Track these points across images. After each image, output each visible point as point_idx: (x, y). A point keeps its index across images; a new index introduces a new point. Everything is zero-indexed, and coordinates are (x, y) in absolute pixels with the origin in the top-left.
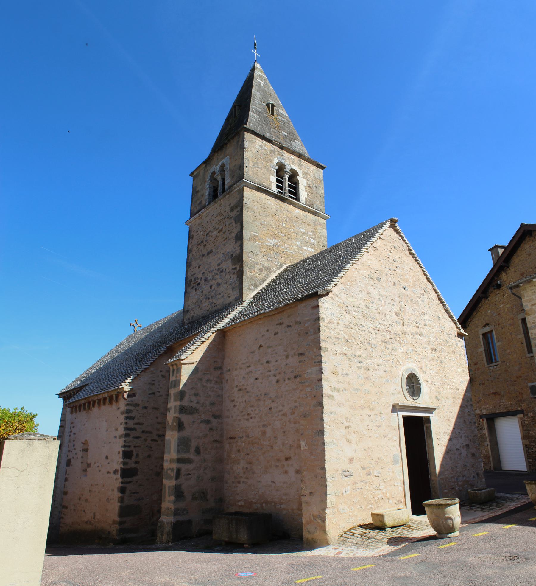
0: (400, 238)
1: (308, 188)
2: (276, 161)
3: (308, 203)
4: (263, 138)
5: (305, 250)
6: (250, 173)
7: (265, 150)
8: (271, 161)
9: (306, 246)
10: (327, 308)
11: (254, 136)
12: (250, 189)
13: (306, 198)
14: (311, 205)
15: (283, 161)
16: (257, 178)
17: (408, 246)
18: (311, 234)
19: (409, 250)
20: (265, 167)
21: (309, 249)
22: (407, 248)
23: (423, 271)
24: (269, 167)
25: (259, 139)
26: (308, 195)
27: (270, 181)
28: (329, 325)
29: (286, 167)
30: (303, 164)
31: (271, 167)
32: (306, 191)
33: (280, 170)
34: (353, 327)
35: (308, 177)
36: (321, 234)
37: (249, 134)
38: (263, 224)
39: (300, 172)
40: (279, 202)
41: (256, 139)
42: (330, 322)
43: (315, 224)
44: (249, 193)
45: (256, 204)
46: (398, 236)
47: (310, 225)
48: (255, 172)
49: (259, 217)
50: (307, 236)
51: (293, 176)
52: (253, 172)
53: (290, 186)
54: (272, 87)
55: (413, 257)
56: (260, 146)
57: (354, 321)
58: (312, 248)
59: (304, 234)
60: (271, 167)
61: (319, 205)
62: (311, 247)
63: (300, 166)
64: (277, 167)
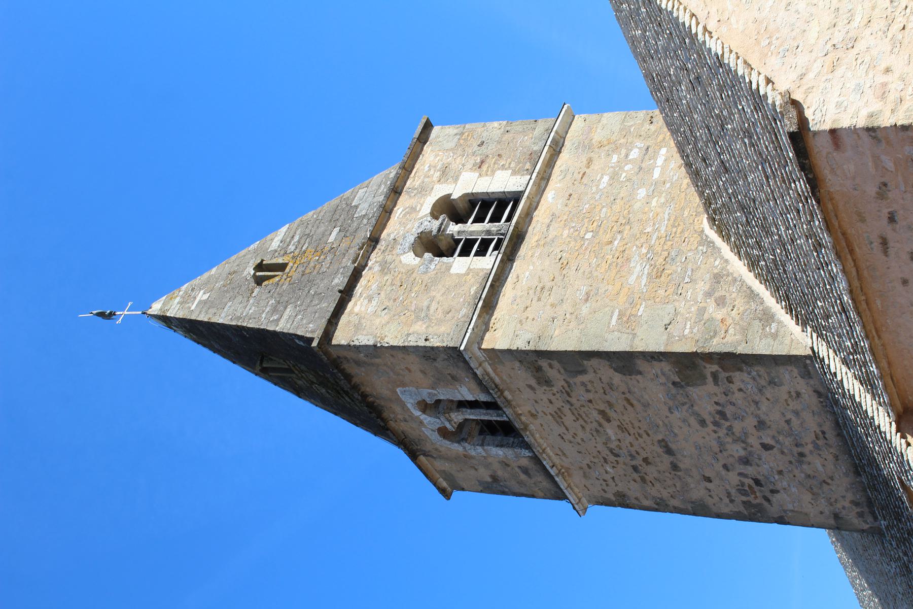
1: (484, 167)
2: (410, 259)
3: (528, 166)
4: (347, 294)
5: (662, 173)
6: (443, 329)
7: (380, 288)
8: (411, 271)
9: (650, 171)
10: (838, 105)
12: (487, 330)
13: (514, 173)
14: (533, 158)
15: (411, 239)
16: (458, 311)
18: (615, 158)
21: (660, 162)
24: (425, 278)
26: (503, 167)
27: (467, 274)
28: (892, 97)
29: (428, 228)
30: (417, 183)
32: (493, 172)
33: (434, 246)
34: (896, 26)
37: (337, 333)
39: (440, 191)
40: (524, 250)
41: (351, 312)
42: (883, 96)
43: (586, 146)
44: (498, 334)
45: (530, 313)
47: (590, 161)
48: (440, 314)
49: (567, 307)
50: (621, 168)
51: (452, 209)
52: (440, 322)
53: (479, 219)
56: (370, 301)
57: (878, 24)
59: (614, 177)
60: (426, 273)
62: (654, 158)
63: (423, 190)
64: (428, 255)
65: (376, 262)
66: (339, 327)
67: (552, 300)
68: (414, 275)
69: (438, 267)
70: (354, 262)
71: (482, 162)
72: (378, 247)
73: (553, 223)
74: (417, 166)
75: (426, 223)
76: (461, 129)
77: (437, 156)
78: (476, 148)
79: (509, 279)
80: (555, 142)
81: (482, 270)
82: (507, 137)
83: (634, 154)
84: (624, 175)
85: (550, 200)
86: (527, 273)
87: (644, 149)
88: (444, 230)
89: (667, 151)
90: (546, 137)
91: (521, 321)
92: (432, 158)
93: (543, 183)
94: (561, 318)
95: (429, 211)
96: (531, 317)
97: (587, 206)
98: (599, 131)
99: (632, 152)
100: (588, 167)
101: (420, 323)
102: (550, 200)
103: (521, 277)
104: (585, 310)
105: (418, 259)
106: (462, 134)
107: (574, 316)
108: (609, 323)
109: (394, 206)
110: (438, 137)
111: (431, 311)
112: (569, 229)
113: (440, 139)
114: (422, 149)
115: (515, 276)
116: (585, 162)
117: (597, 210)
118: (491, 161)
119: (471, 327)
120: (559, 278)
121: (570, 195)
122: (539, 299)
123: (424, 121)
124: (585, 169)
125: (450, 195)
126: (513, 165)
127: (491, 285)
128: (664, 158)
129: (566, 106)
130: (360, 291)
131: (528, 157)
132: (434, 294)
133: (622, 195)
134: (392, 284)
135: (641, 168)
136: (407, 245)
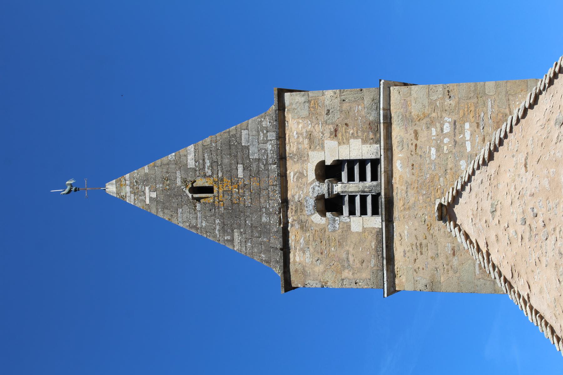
0: (468, 188)
1: (339, 135)
2: (317, 218)
3: (371, 135)
4: (286, 249)
7: (307, 243)
8: (323, 230)
9: (463, 145)
11: (292, 268)
12: (394, 276)
13: (364, 142)
14: (374, 127)
15: (312, 202)
16: (370, 262)
17: (478, 168)
18: (434, 131)
19: (485, 163)
20: (340, 244)
21: (468, 136)
22: (483, 168)
23: (518, 121)
24: (336, 235)
25: (291, 255)
26: (354, 136)
30: (294, 149)
31: (334, 231)
32: (348, 140)
33: (331, 205)
35: (315, 134)
36: (426, 103)
37: (293, 278)
38: (453, 249)
39: (315, 158)
40: (396, 214)
41: (295, 261)
43: (408, 119)
44: (404, 279)
45: (418, 264)
46: (465, 194)
47: (416, 133)
48: (358, 265)
50: (442, 141)
51: (329, 172)
53: (351, 178)
54: (142, 165)
55: (496, 149)
56: (304, 252)
58: (462, 127)
59: (439, 149)
61: (362, 105)
62: (462, 132)
63: (302, 157)
64: (328, 214)
65: (294, 220)
66: (291, 274)
67: (430, 254)
68: (327, 233)
69: (341, 226)
70: (280, 224)
71: (336, 131)
72: (290, 206)
73: (409, 189)
74: (287, 132)
75: (317, 188)
76: (306, 96)
77: (298, 123)
78: (326, 117)
79: (395, 237)
80: (385, 117)
81: (374, 228)
82: (345, 106)
83: (447, 128)
84: (445, 148)
86: (406, 232)
87: (452, 123)
88: (332, 192)
89: (470, 126)
90: (374, 107)
91: (415, 270)
92: (296, 125)
93: (389, 153)
94: (441, 267)
96: (421, 268)
97: (428, 176)
98: (413, 104)
99: (445, 127)
100: (417, 140)
101: (347, 271)
103: (403, 235)
104: (455, 262)
105: (324, 219)
106: (309, 102)
107: (449, 267)
108: (475, 272)
109: (286, 170)
110: (291, 104)
111: (351, 262)
112: (423, 196)
113: (294, 106)
114: (284, 117)
115: (398, 235)
116: (413, 135)
117: (436, 179)
118: (342, 129)
119: (385, 280)
120: (429, 237)
121: (413, 165)
122: (421, 254)
124: (415, 142)
125: (323, 162)
126: (360, 134)
127: (387, 246)
128: (469, 132)
129: (382, 82)
130: (293, 244)
131: (368, 126)
132: (347, 248)
133: (450, 166)
134: (314, 240)
135: (455, 142)
136: (311, 208)
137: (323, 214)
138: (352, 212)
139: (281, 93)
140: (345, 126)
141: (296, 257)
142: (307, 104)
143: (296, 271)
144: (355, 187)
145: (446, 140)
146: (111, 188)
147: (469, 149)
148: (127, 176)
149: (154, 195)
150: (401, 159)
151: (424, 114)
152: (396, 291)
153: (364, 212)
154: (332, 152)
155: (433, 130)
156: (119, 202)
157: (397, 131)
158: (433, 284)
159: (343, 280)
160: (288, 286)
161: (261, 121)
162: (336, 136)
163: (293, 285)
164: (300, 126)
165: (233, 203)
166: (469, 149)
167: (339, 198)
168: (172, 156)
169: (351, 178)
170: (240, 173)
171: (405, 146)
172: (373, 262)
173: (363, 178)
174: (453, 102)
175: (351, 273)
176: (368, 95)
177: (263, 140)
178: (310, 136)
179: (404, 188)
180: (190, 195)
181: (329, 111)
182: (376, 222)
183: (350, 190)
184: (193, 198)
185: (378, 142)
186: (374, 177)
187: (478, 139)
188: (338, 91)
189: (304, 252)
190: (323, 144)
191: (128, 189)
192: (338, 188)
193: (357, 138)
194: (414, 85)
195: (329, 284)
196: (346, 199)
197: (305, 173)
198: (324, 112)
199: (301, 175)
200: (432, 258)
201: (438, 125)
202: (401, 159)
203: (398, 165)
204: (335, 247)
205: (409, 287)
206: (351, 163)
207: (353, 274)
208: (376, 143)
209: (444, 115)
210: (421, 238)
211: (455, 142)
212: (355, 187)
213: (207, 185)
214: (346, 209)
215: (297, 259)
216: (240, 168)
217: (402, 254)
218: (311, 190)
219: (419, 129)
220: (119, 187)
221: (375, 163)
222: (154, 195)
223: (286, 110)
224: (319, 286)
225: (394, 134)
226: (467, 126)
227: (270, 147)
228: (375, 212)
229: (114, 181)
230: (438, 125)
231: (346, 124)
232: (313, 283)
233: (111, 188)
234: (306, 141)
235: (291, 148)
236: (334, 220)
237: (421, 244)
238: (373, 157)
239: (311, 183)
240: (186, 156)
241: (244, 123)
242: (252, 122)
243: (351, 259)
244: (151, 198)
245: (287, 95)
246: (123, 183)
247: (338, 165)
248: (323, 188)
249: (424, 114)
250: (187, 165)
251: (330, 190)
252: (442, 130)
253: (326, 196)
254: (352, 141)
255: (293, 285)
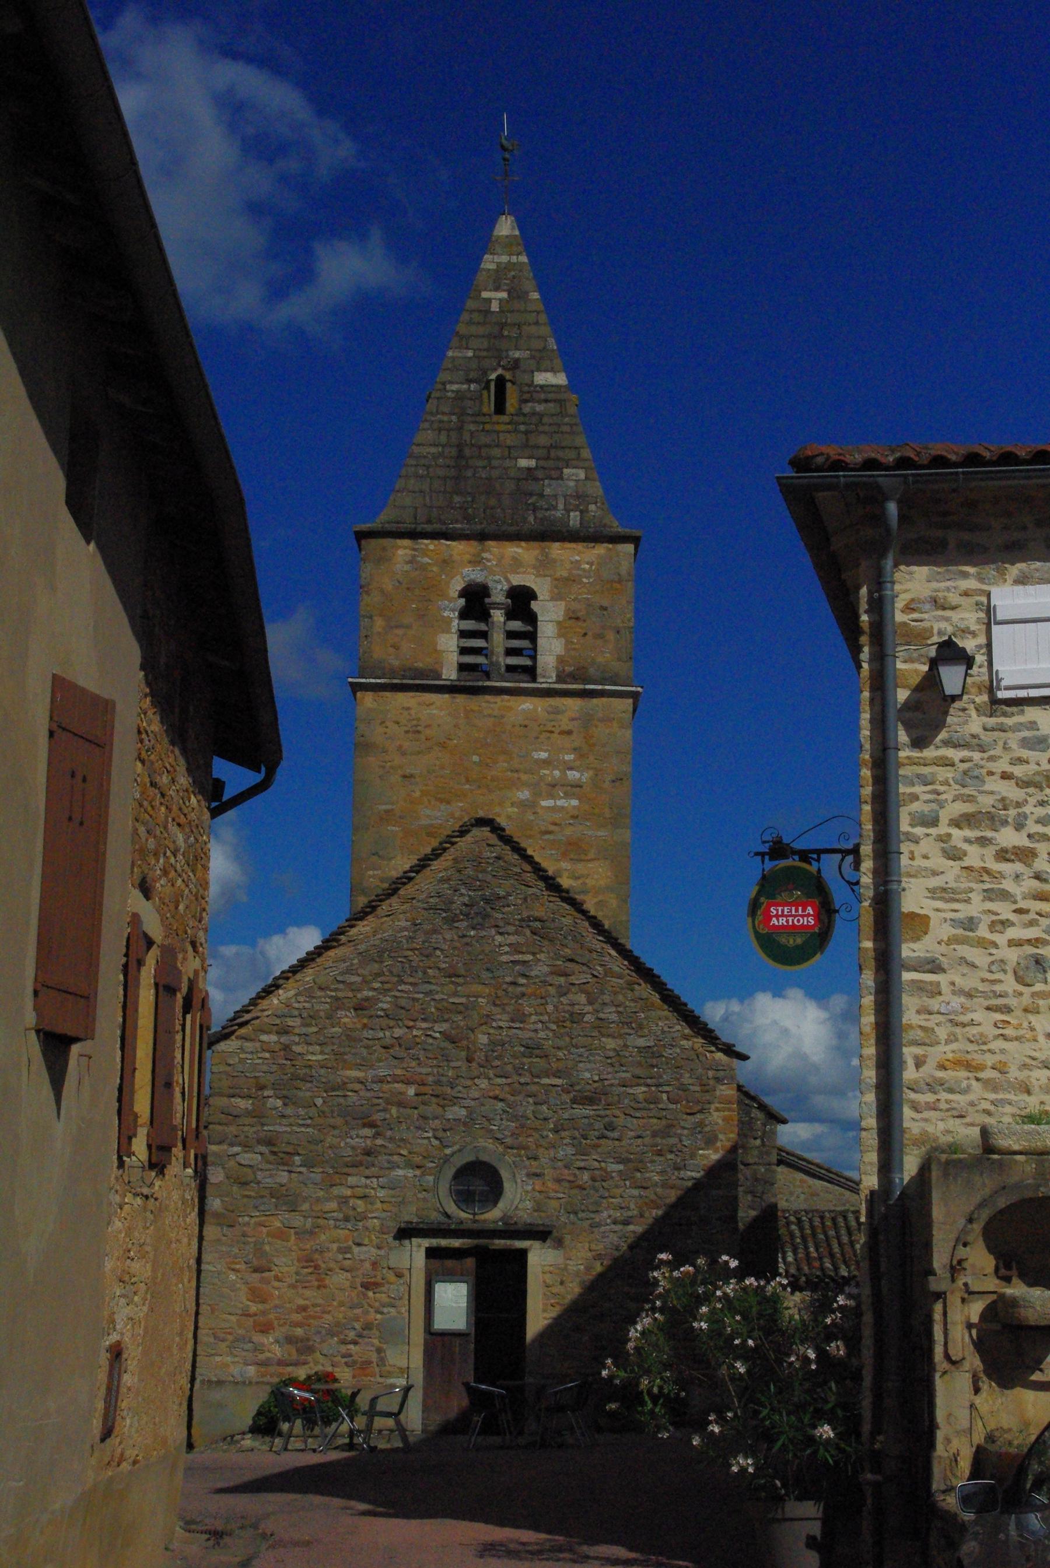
2: (457, 585)
3: (568, 669)
9: (551, 796)
13: (561, 660)
26: (568, 642)
29: (493, 592)
38: (412, 776)
39: (541, 587)
40: (461, 699)
47: (569, 733)
50: (556, 768)
56: (410, 562)
59: (546, 763)
62: (567, 796)
63: (544, 565)
71: (577, 619)
73: (493, 719)
75: (499, 587)
77: (591, 564)
82: (611, 636)
83: (573, 775)
85: (523, 706)
88: (494, 608)
89: (574, 807)
95: (515, 583)
102: (523, 706)
104: (395, 778)
106: (620, 581)
116: (566, 728)
122: (407, 732)
123: (637, 533)
129: (639, 689)
135: (554, 786)
136: (472, 577)
137: (463, 593)
138: (463, 634)
139: (636, 540)
140: (583, 632)
141: (402, 550)
142: (616, 578)
143: (384, 549)
144: (499, 641)
145: (557, 773)
146: (505, 227)
147: (544, 803)
148: (524, 259)
149: (495, 307)
150: (535, 710)
151: (594, 745)
152: (354, 693)
153: (464, 651)
154: (549, 613)
155: (572, 757)
156: (485, 242)
157: (573, 705)
158: (366, 747)
159: (371, 617)
160: (361, 536)
161: (596, 503)
162: (570, 618)
163: (363, 542)
164: (587, 566)
165: (480, 447)
166: (544, 803)
167: (484, 615)
168: (552, 344)
169: (511, 635)
170: (523, 463)
171: (552, 716)
172: (396, 663)
173: (510, 652)
174: (607, 785)
175: (380, 630)
176: (623, 668)
177: (570, 504)
178: (570, 580)
179: (496, 713)
180: (493, 376)
181: (605, 609)
182: (450, 674)
183: (495, 635)
184: (489, 382)
185: (560, 679)
186: (510, 669)
187: (557, 817)
188: (632, 624)
189: (410, 562)
190: (561, 599)
191: (504, 259)
192: (498, 616)
193: (567, 650)
194: (634, 710)
195: (365, 596)
196: (483, 627)
197: (522, 570)
198: (605, 603)
199: (517, 564)
200: (400, 746)
201: (578, 763)
202: (535, 710)
203: (527, 704)
204: (418, 609)
205: (360, 711)
206: (532, 636)
207: (379, 633)
208: (558, 676)
209: (591, 773)
210: (428, 732)
211: (554, 786)
212: (499, 641)
213: (508, 405)
214: (470, 625)
215: (400, 552)
216: (532, 463)
217: (406, 705)
218: (497, 578)
219: (574, 737)
220: (508, 243)
221: (531, 672)
222: (495, 307)
223: (610, 546)
224: (363, 582)
225: (569, 702)
226: (575, 802)
227: (559, 514)
228: (462, 667)
229: (517, 233)
230: (578, 763)
231: (585, 634)
232: (367, 570)
233: (505, 227)
234: (565, 574)
235: (556, 549)
236: (453, 610)
237: (419, 732)
238: (539, 671)
239: (507, 580)
240: (552, 370)
241: (596, 476)
242: (596, 489)
243: (400, 632)
244: (489, 300)
245: (630, 548)
246: (515, 249)
247: (532, 619)
248: (498, 595)
249: (594, 745)
250: (539, 370)
251: (497, 606)
252: (571, 769)
253: (487, 600)
254: (563, 640)
255: (363, 542)
